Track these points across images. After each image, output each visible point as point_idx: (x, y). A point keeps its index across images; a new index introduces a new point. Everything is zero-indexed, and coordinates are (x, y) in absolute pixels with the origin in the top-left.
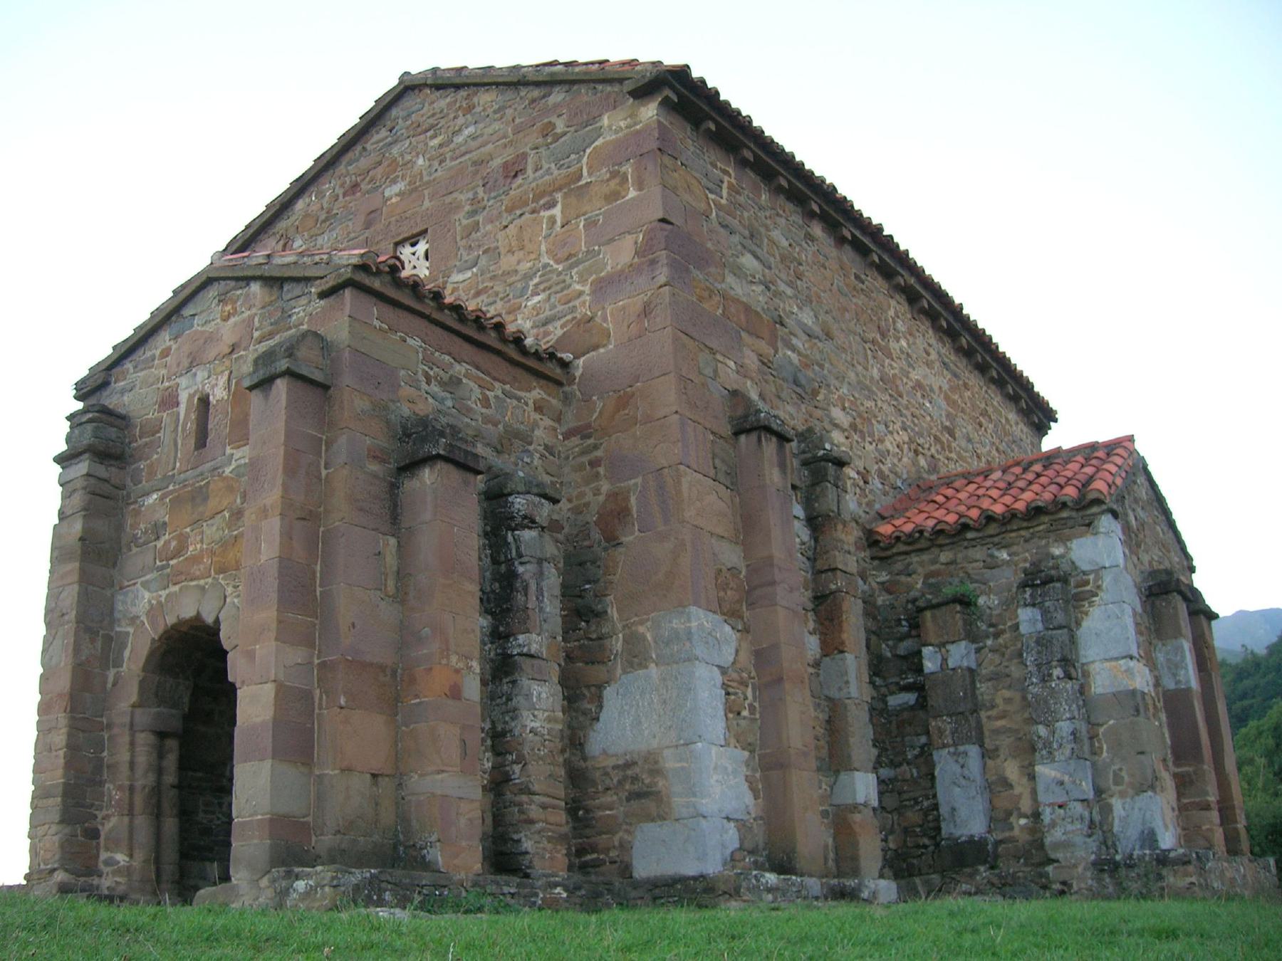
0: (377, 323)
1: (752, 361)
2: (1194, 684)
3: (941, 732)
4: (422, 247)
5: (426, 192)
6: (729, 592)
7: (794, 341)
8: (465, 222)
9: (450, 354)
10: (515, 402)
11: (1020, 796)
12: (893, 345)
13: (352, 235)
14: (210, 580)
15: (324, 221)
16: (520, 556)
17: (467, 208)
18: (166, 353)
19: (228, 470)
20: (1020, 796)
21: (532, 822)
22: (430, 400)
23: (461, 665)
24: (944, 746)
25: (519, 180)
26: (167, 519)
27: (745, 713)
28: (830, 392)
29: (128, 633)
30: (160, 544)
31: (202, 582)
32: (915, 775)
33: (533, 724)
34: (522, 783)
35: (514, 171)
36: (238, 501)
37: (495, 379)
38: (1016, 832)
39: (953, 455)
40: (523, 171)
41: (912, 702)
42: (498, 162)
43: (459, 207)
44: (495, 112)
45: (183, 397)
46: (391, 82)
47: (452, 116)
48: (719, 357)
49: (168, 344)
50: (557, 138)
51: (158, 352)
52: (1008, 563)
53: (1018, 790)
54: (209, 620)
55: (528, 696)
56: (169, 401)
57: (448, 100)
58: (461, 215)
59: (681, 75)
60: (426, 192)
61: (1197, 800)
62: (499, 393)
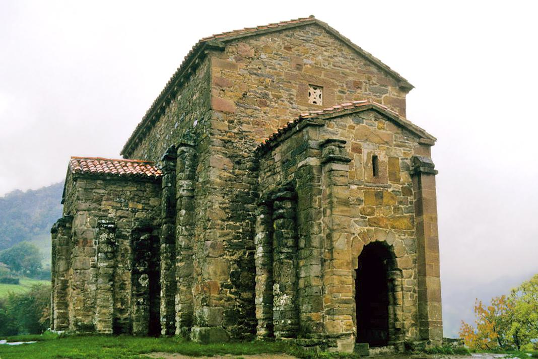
4: (318, 92)
5: (323, 72)
13: (289, 69)
14: (388, 230)
15: (274, 54)
17: (339, 88)
18: (353, 128)
19: (390, 190)
25: (359, 91)
26: (363, 198)
30: (360, 207)
31: (384, 229)
35: (357, 85)
36: (397, 204)
40: (361, 88)
42: (350, 78)
43: (337, 86)
45: (365, 151)
46: (306, 15)
47: (333, 48)
49: (352, 123)
50: (374, 84)
51: (348, 125)
54: (390, 244)
56: (357, 149)
58: (336, 90)
60: (323, 72)
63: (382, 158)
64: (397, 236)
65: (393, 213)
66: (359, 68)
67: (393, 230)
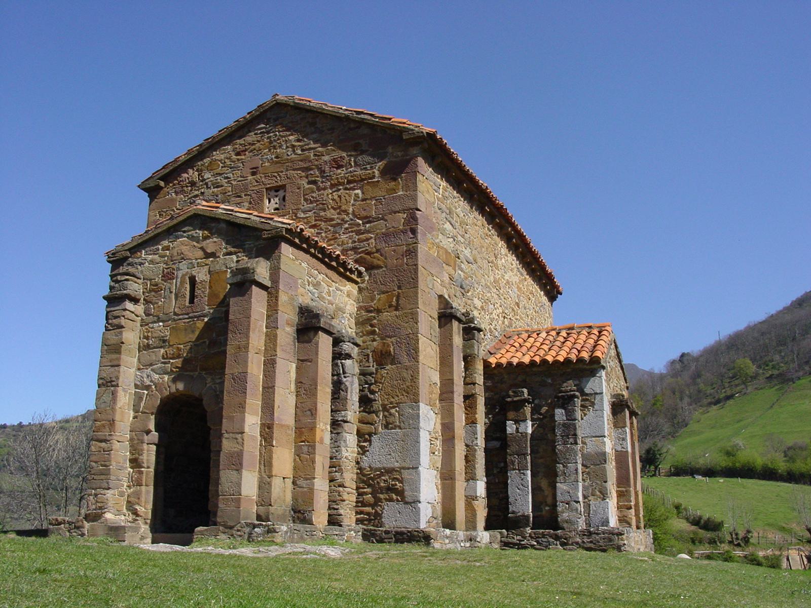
0: (291, 256)
1: (446, 278)
2: (629, 450)
3: (513, 463)
6: (433, 395)
7: (463, 266)
8: (307, 186)
9: (317, 270)
10: (340, 292)
11: (547, 496)
12: (499, 262)
14: (197, 373)
16: (344, 372)
20: (547, 496)
21: (344, 501)
22: (310, 294)
23: (324, 428)
24: (515, 469)
27: (436, 453)
28: (475, 291)
29: (144, 393)
31: (192, 374)
32: (497, 481)
33: (346, 454)
34: (340, 482)
36: (214, 335)
37: (333, 281)
38: (544, 513)
39: (518, 317)
41: (498, 446)
44: (329, 130)
48: (435, 278)
51: (160, 247)
52: (551, 385)
53: (546, 493)
54: (197, 394)
55: (345, 441)
57: (301, 116)
59: (431, 136)
61: (626, 504)
62: (334, 289)
63: (202, 276)
64: (209, 380)
65: (207, 350)
66: (341, 138)
67: (204, 372)
